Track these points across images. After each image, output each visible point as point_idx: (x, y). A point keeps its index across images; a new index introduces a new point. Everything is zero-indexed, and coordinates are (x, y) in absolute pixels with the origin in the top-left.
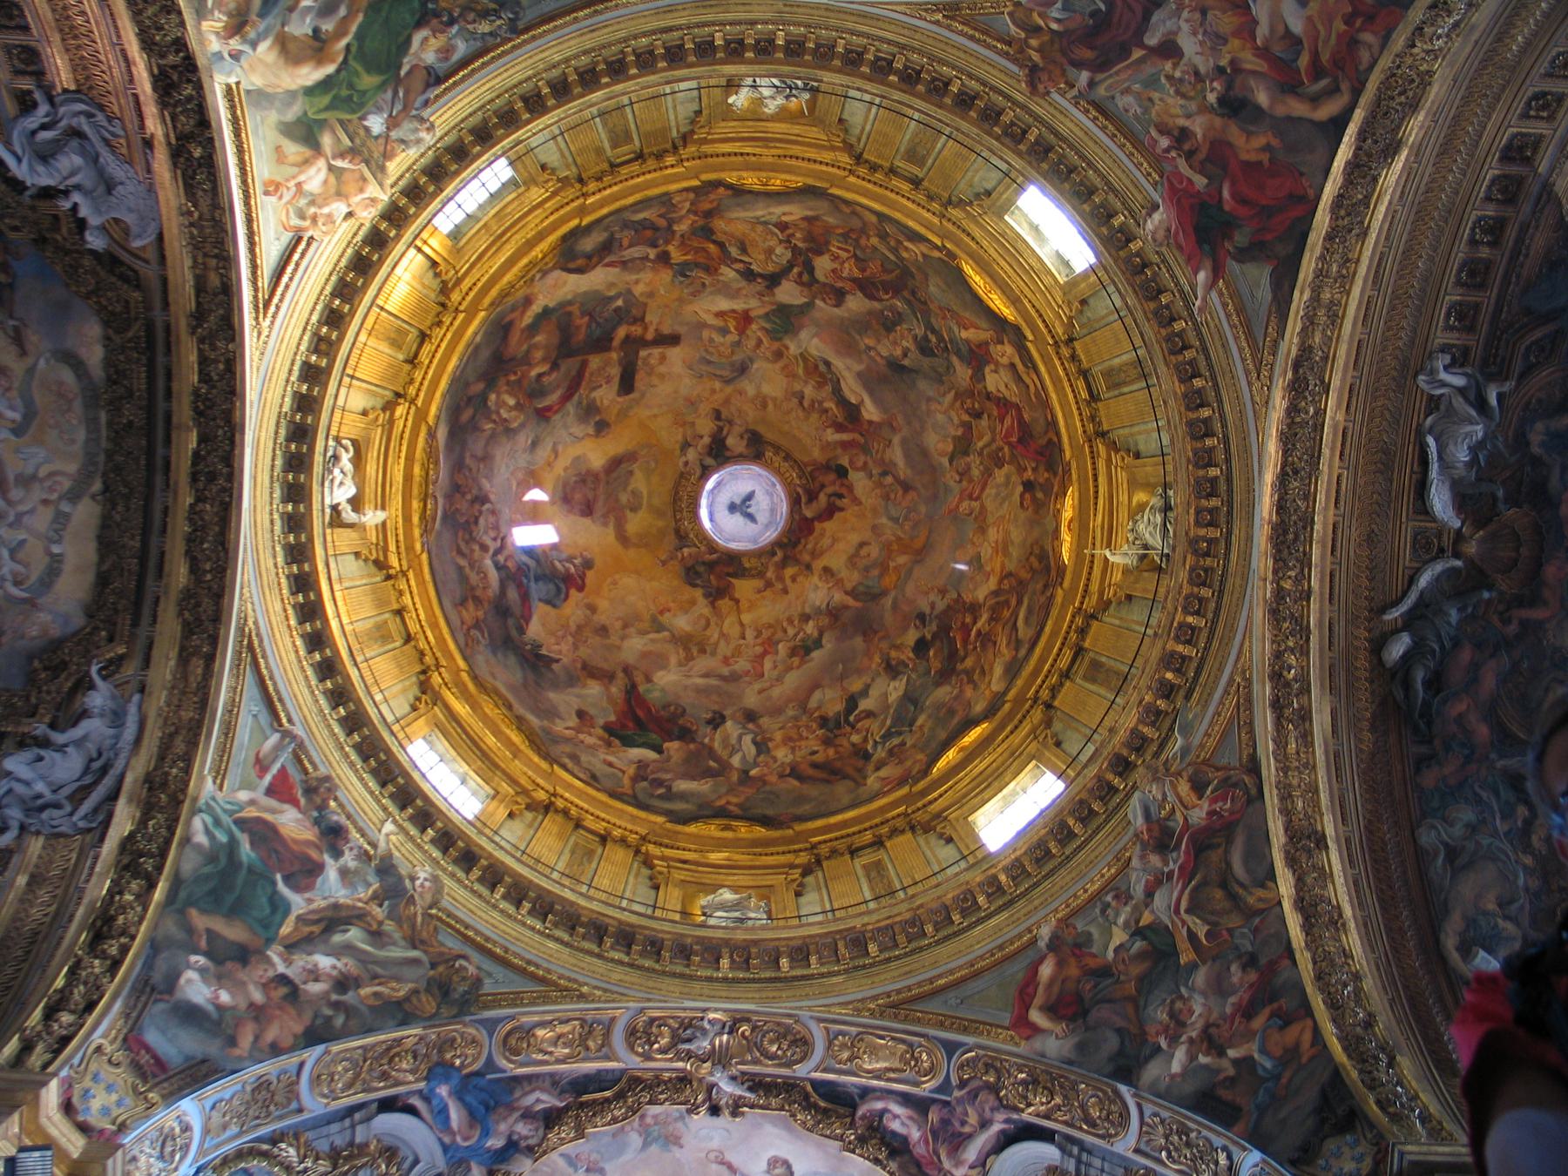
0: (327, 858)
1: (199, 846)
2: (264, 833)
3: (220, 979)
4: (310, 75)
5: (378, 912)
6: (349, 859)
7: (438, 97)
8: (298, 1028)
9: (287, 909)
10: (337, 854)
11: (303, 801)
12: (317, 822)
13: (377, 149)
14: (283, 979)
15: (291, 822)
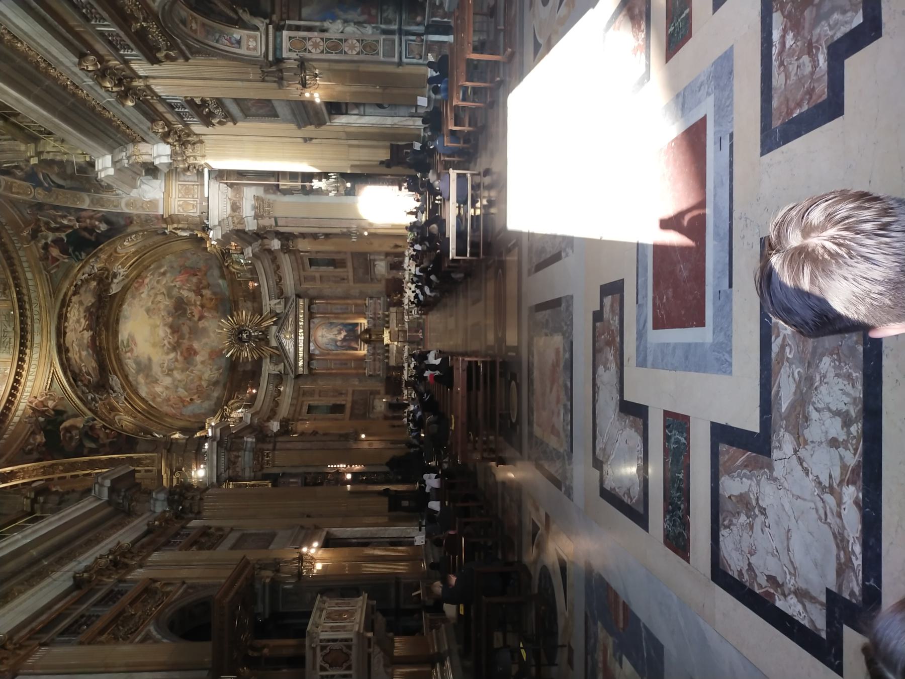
0: (49, 243)
1: (84, 252)
2: (64, 251)
3: (96, 226)
4: (66, 424)
5: (43, 229)
6: (43, 241)
7: (29, 430)
8: (84, 214)
9: (67, 236)
10: (46, 244)
11: (50, 257)
12: (48, 251)
13: (37, 414)
14: (78, 221)
15: (55, 252)
